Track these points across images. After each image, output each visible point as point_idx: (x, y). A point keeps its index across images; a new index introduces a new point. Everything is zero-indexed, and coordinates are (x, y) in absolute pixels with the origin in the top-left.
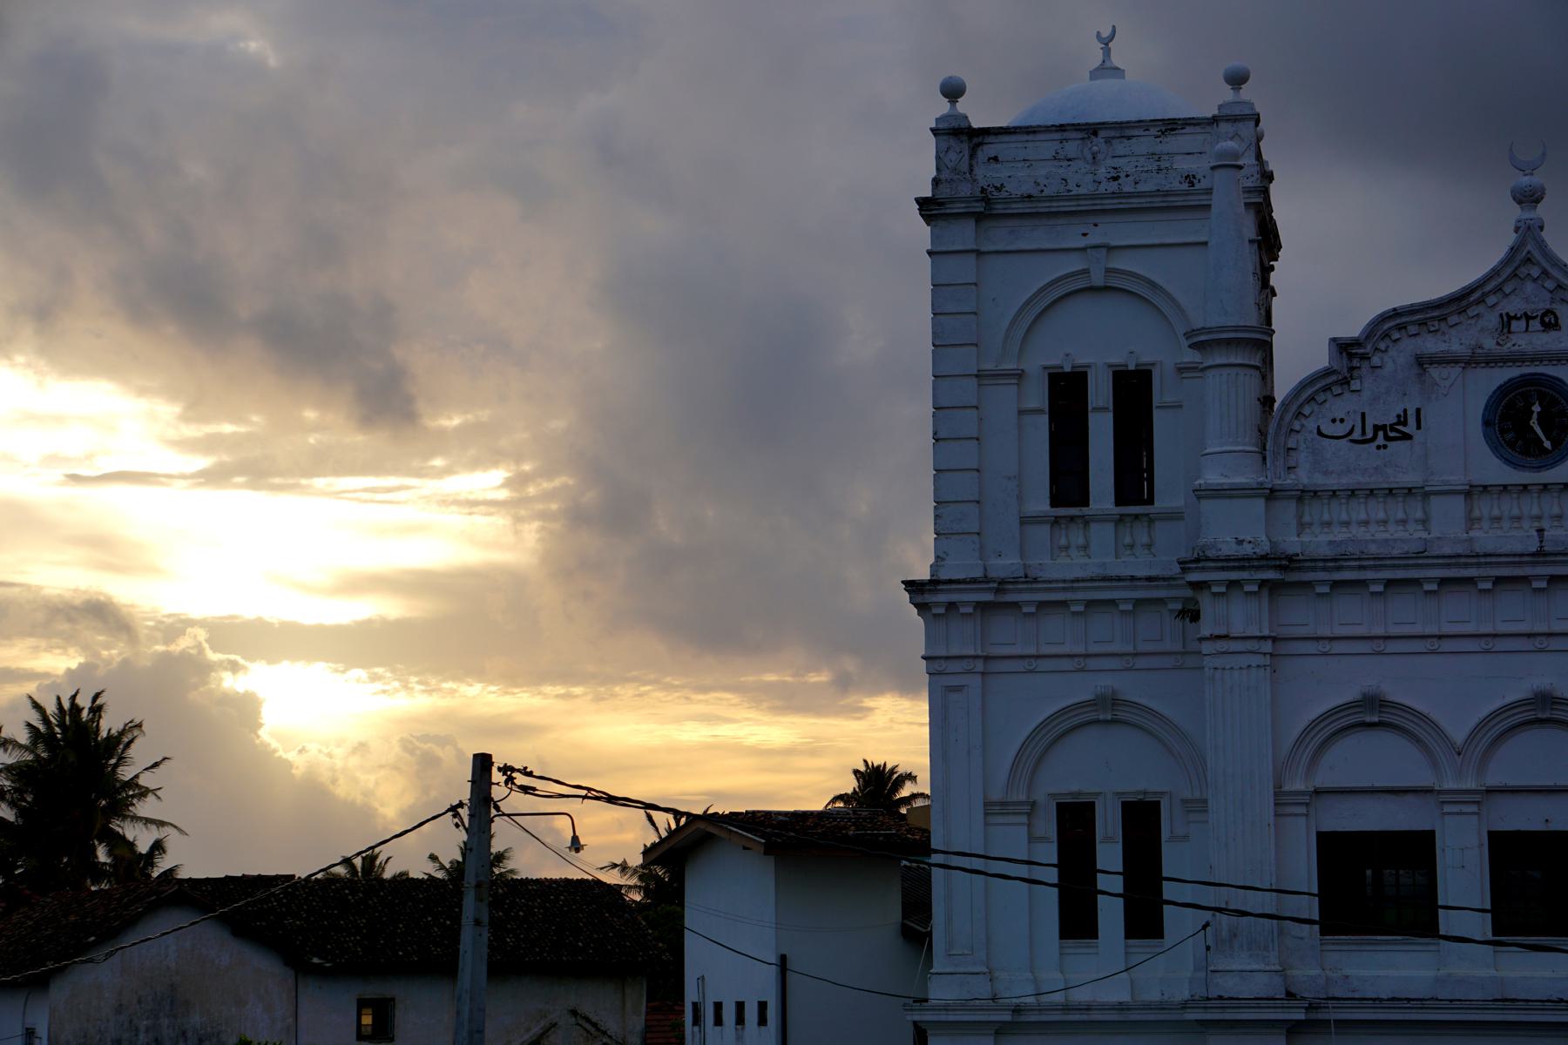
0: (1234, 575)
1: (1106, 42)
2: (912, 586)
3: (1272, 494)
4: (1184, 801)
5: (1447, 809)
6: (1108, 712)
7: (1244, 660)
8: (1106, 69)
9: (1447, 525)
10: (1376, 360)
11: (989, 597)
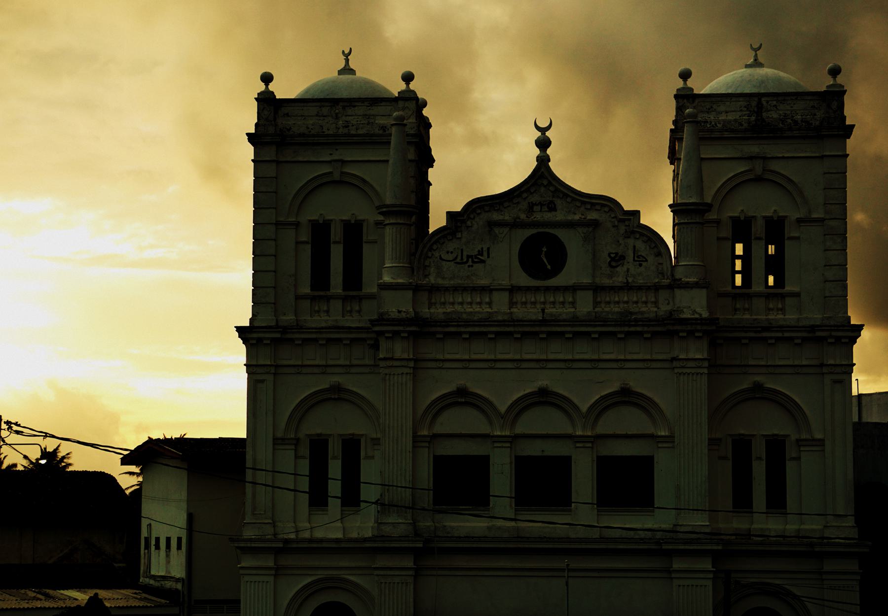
0: (396, 328)
1: (347, 56)
2: (240, 329)
4: (372, 439)
6: (337, 395)
7: (400, 371)
8: (347, 70)
9: (500, 304)
10: (469, 223)
11: (278, 335)
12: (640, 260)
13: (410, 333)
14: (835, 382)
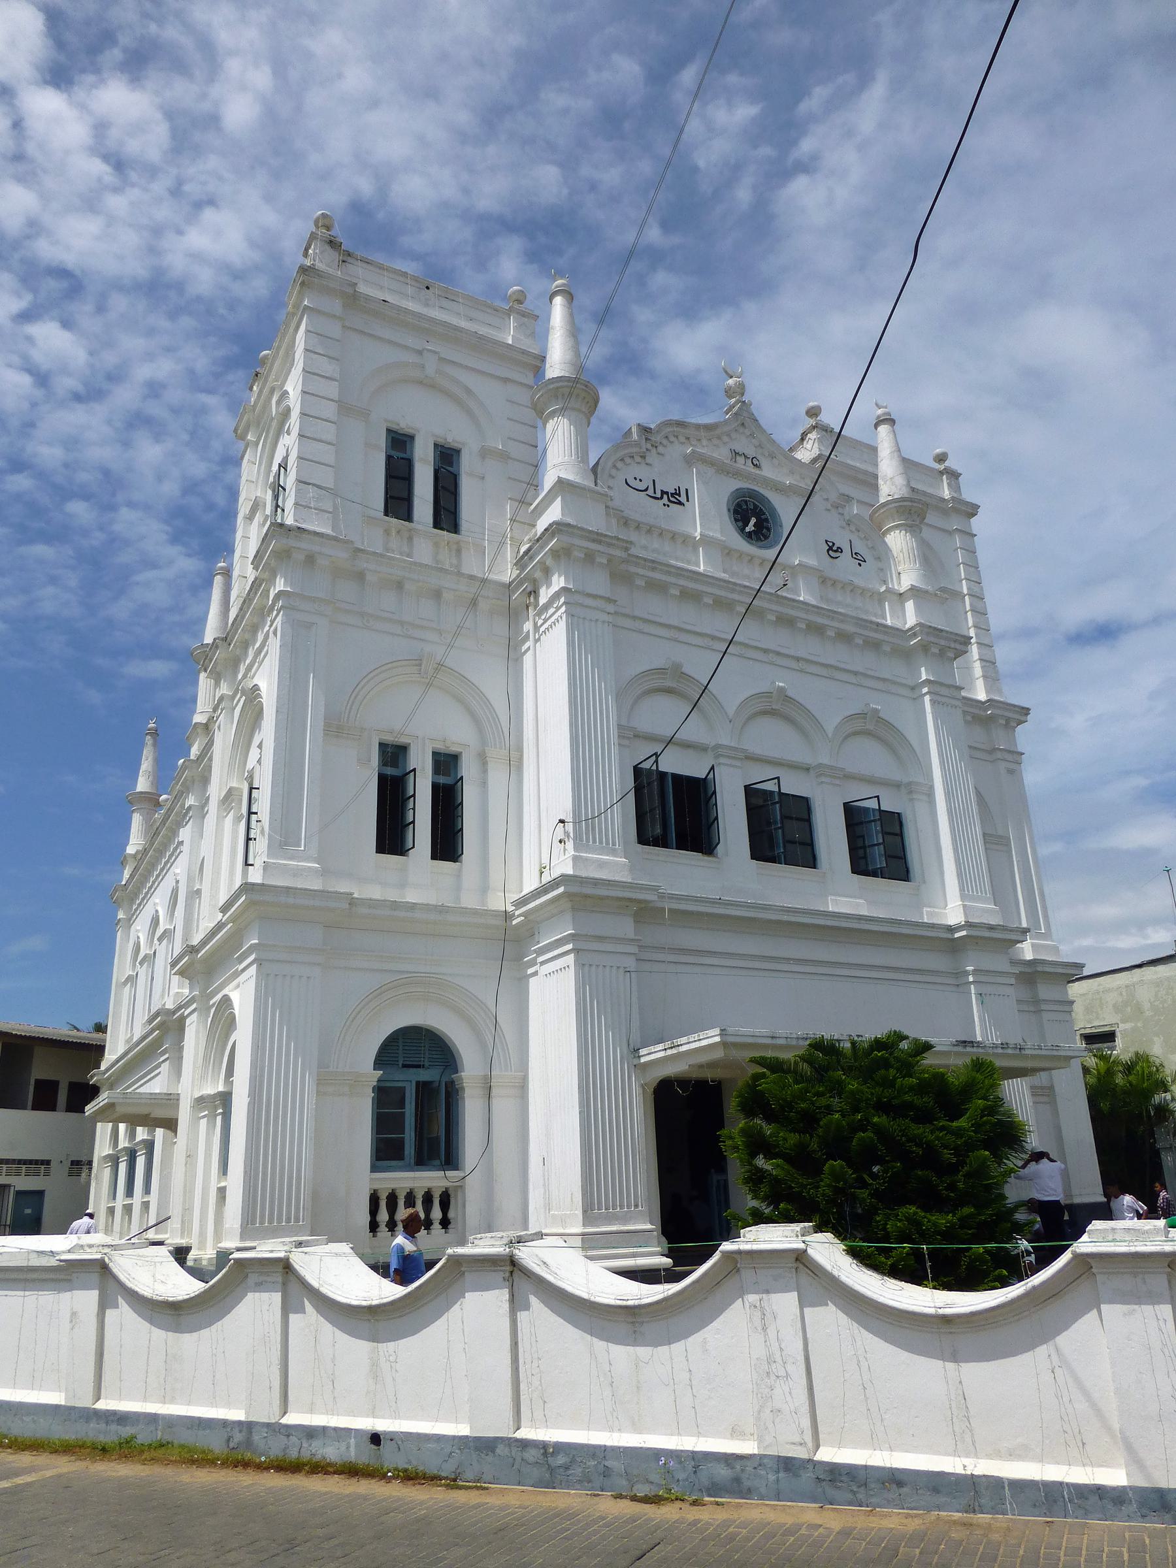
10: (660, 449)
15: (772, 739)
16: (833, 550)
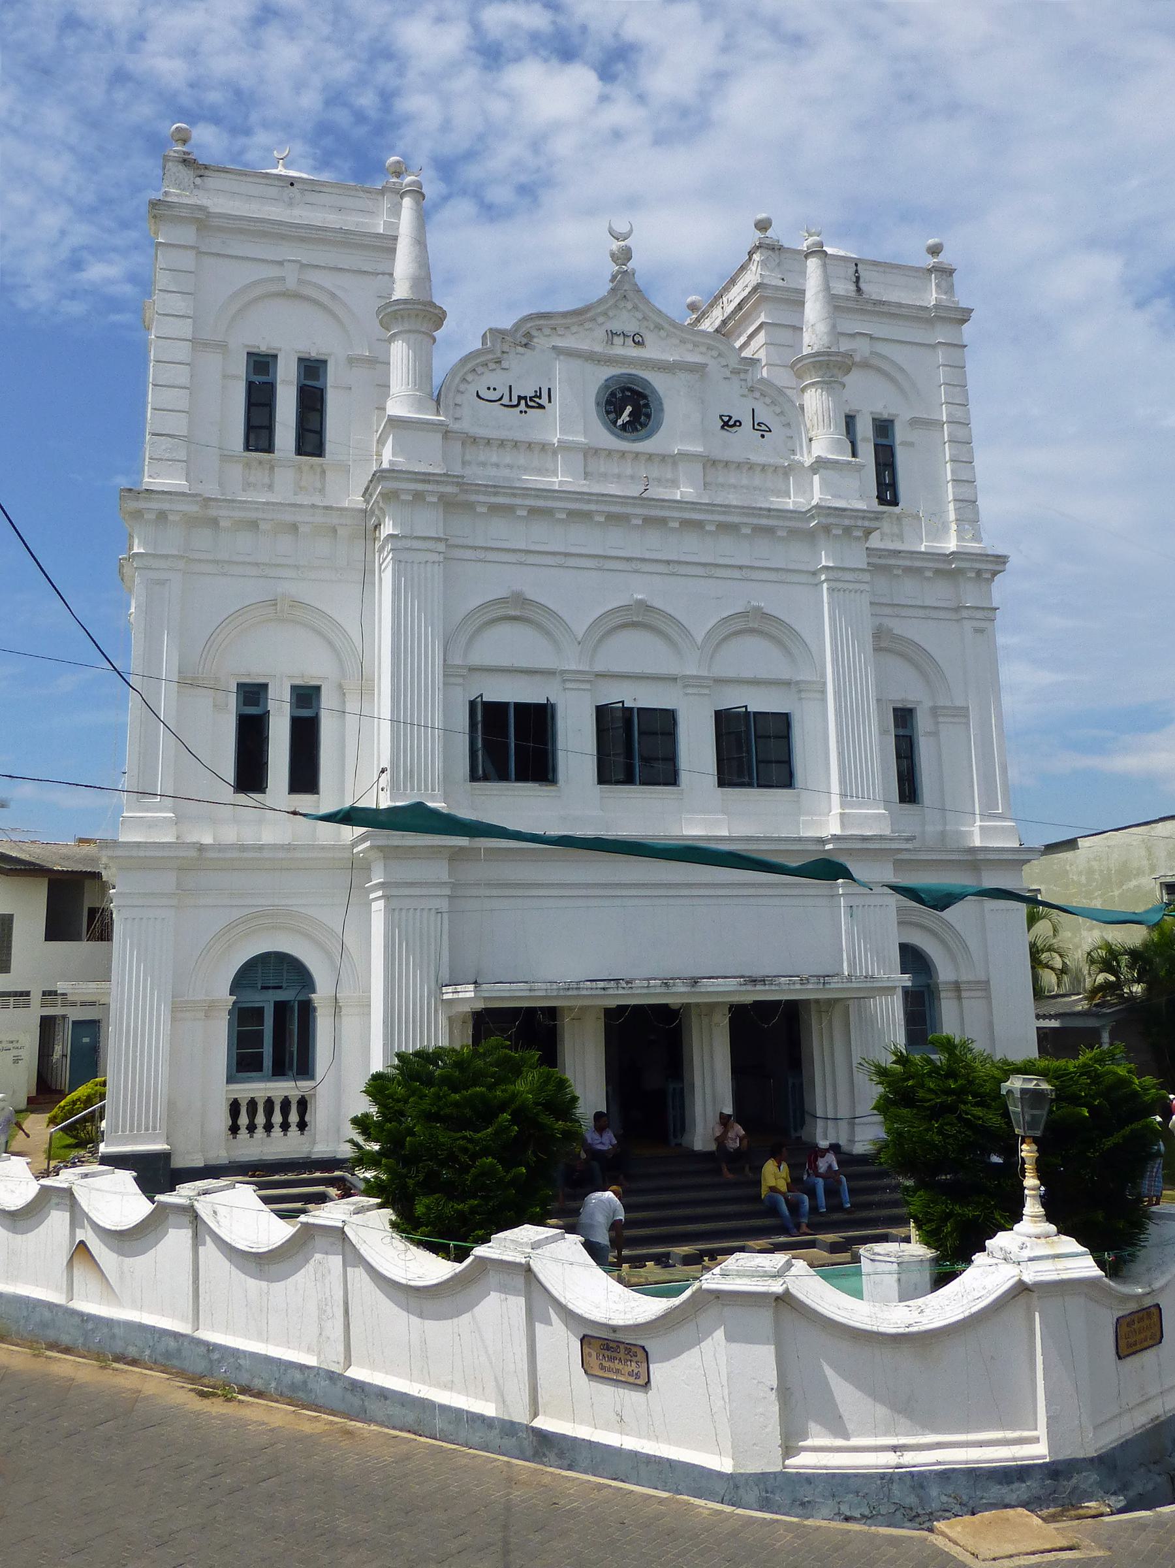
0: (420, 487)
3: (447, 434)
5: (569, 685)
12: (762, 429)
13: (442, 496)
14: (978, 631)
15: (635, 652)
16: (728, 424)
